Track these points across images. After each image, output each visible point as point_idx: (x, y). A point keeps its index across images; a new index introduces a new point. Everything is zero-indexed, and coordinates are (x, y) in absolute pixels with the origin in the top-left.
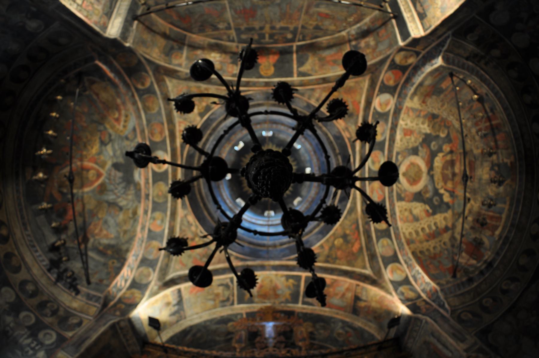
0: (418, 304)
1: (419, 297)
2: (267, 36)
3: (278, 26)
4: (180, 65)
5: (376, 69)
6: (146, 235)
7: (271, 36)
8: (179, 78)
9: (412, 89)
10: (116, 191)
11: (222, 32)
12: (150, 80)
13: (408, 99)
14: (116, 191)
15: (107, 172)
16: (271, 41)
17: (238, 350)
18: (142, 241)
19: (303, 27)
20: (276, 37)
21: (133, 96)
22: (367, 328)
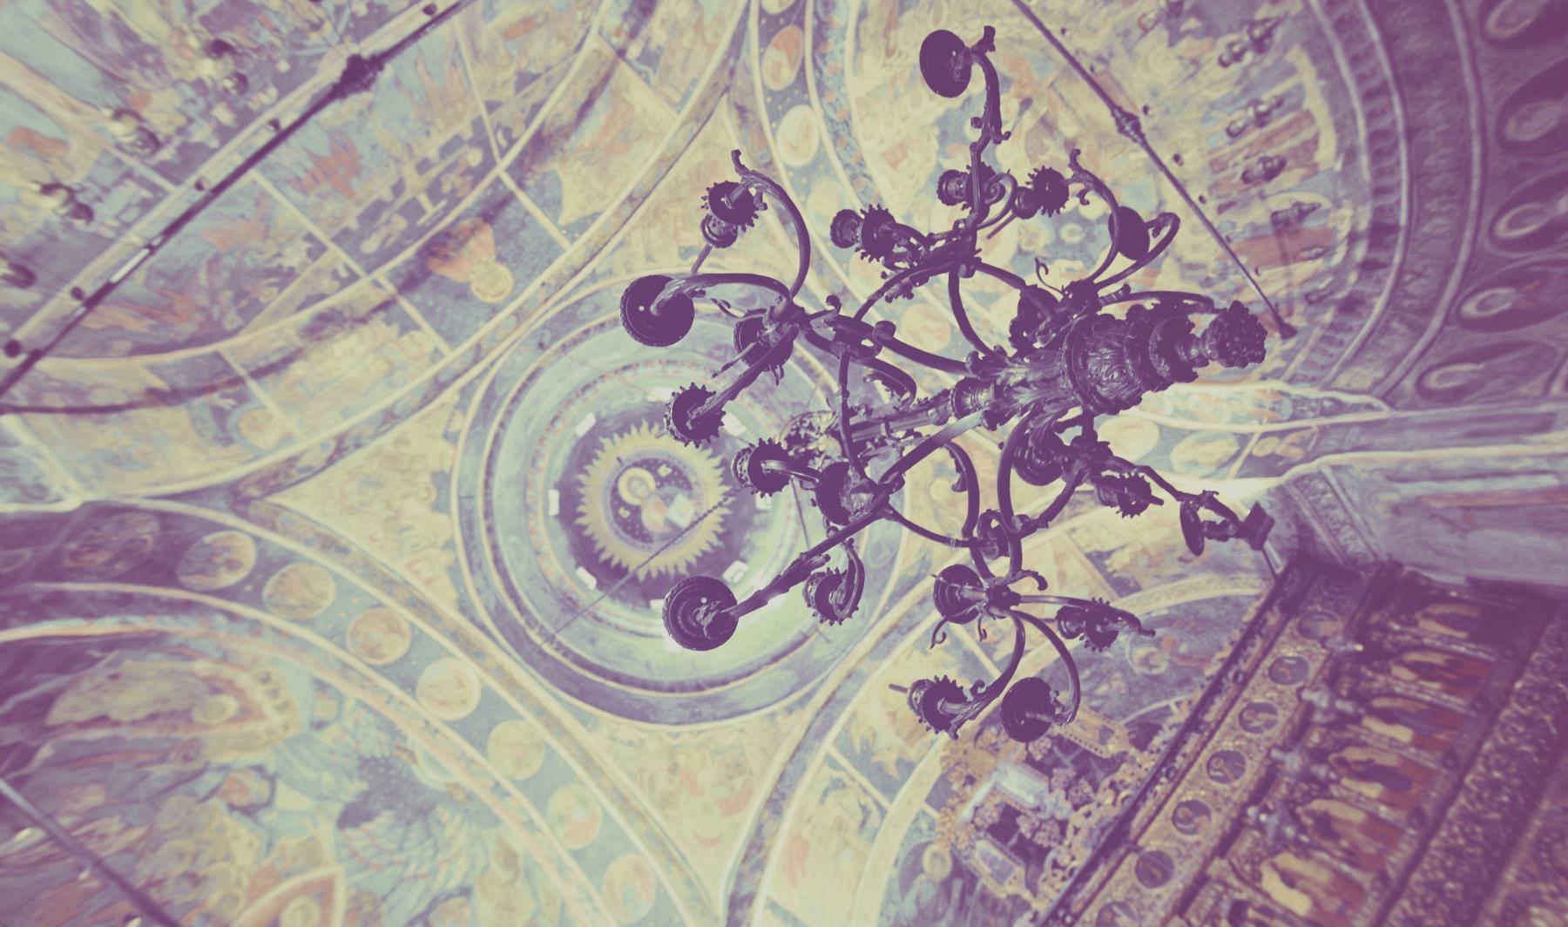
0: (1256, 452)
1: (1243, 439)
2: (424, 200)
3: (432, 153)
4: (288, 438)
5: (732, 72)
6: (583, 877)
7: (434, 192)
8: (312, 472)
9: (849, 45)
10: (411, 870)
11: (307, 273)
12: (242, 540)
13: (849, 78)
14: (411, 870)
15: (340, 860)
16: (443, 203)
17: (1027, 895)
18: (589, 898)
19: (492, 106)
20: (446, 188)
21: (232, 617)
22: (1192, 597)
